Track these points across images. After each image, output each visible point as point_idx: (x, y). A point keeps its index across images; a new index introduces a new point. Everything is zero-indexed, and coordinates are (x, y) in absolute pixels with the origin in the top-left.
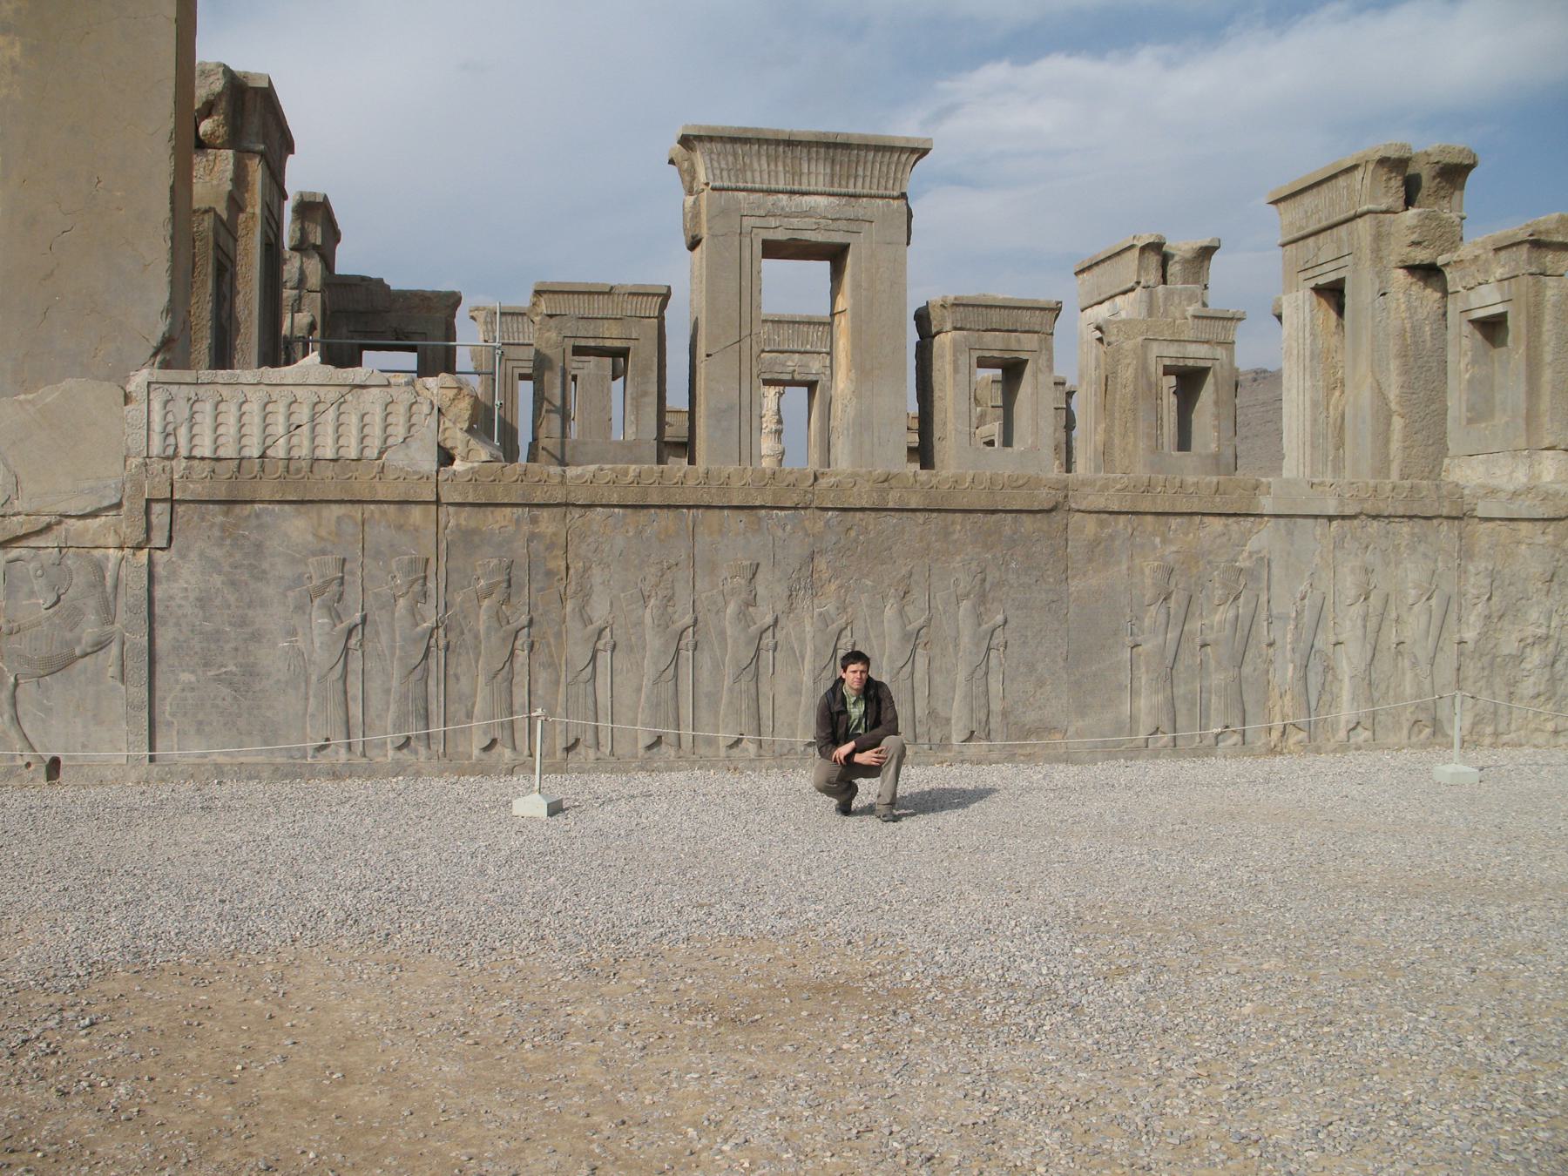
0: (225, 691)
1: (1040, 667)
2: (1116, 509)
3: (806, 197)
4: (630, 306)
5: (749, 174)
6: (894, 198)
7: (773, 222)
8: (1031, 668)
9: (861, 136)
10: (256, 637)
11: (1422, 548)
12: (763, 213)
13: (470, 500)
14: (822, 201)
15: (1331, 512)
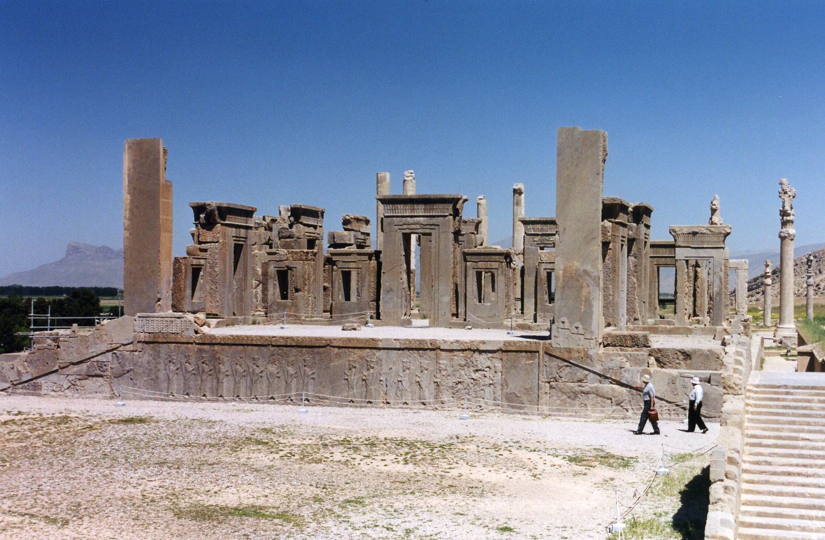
0: (153, 382)
1: (323, 383)
2: (341, 345)
3: (415, 218)
4: (359, 258)
5: (397, 211)
6: (446, 216)
7: (405, 227)
8: (321, 383)
9: (434, 195)
10: (159, 370)
11: (425, 356)
12: (401, 224)
13: (200, 342)
14: (422, 219)
15: (398, 347)
